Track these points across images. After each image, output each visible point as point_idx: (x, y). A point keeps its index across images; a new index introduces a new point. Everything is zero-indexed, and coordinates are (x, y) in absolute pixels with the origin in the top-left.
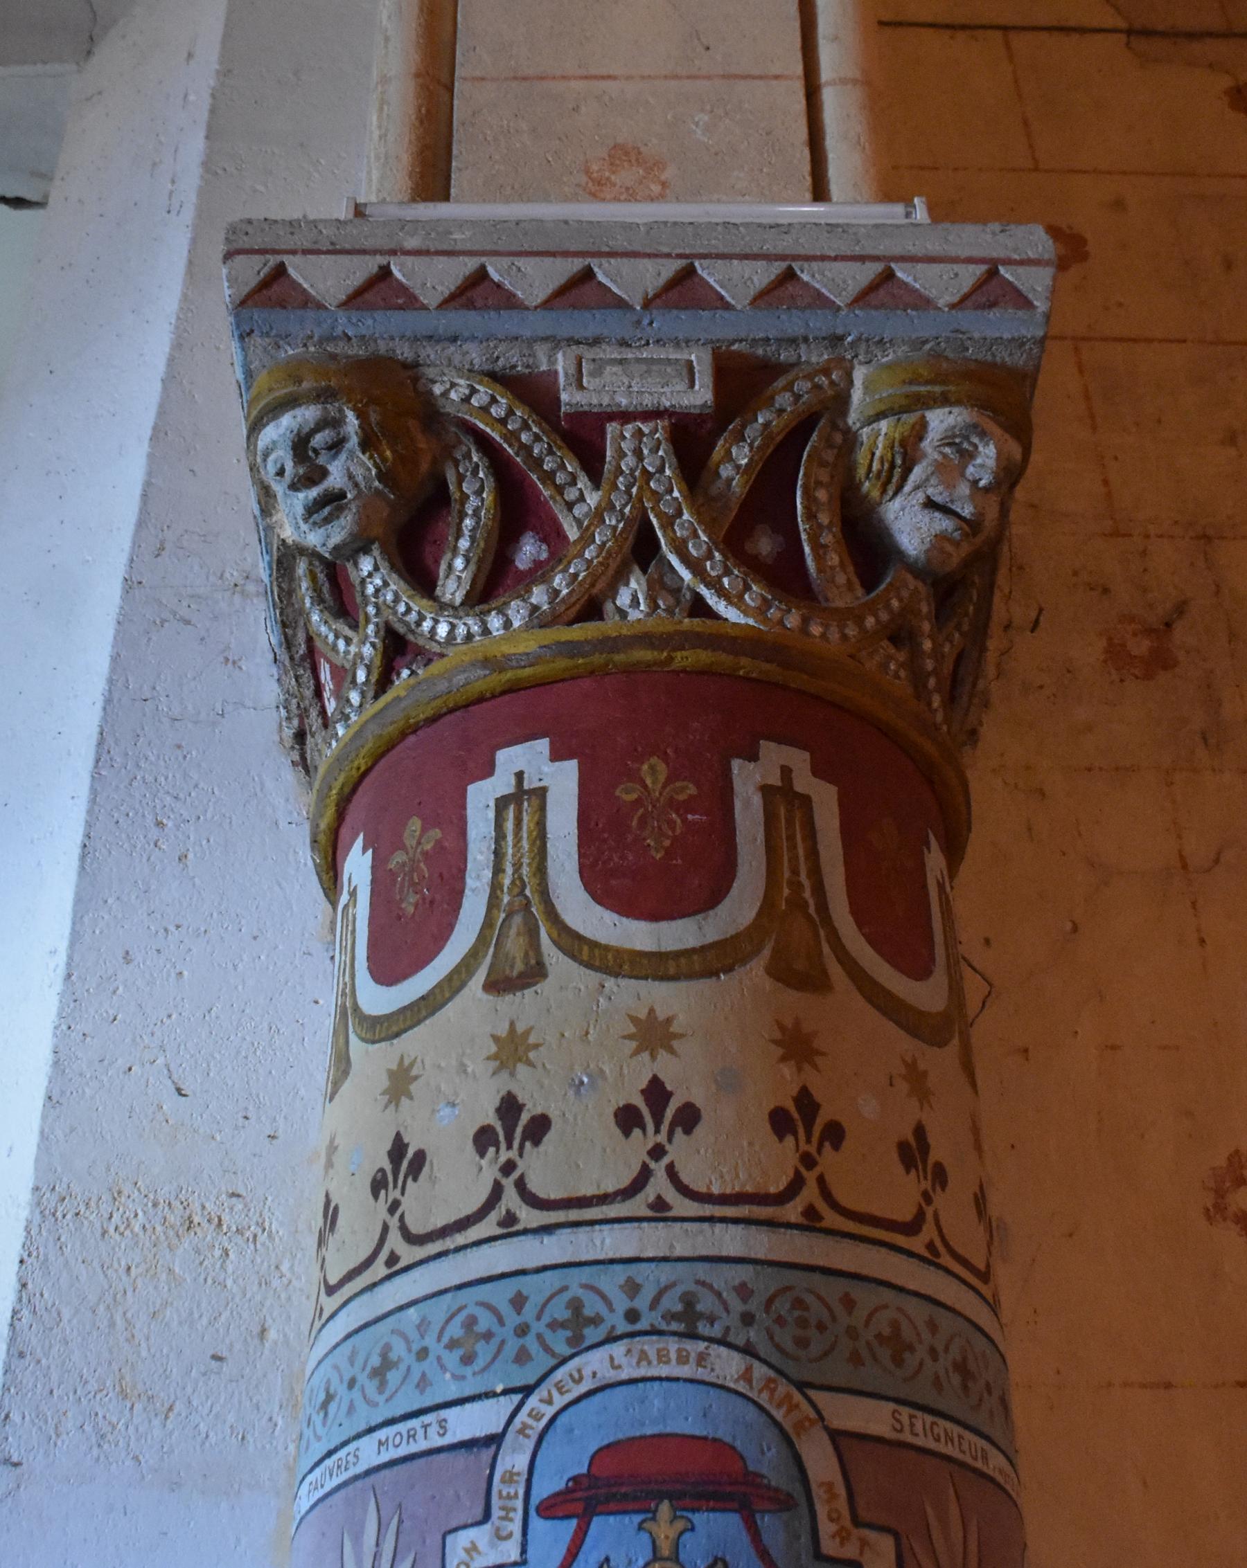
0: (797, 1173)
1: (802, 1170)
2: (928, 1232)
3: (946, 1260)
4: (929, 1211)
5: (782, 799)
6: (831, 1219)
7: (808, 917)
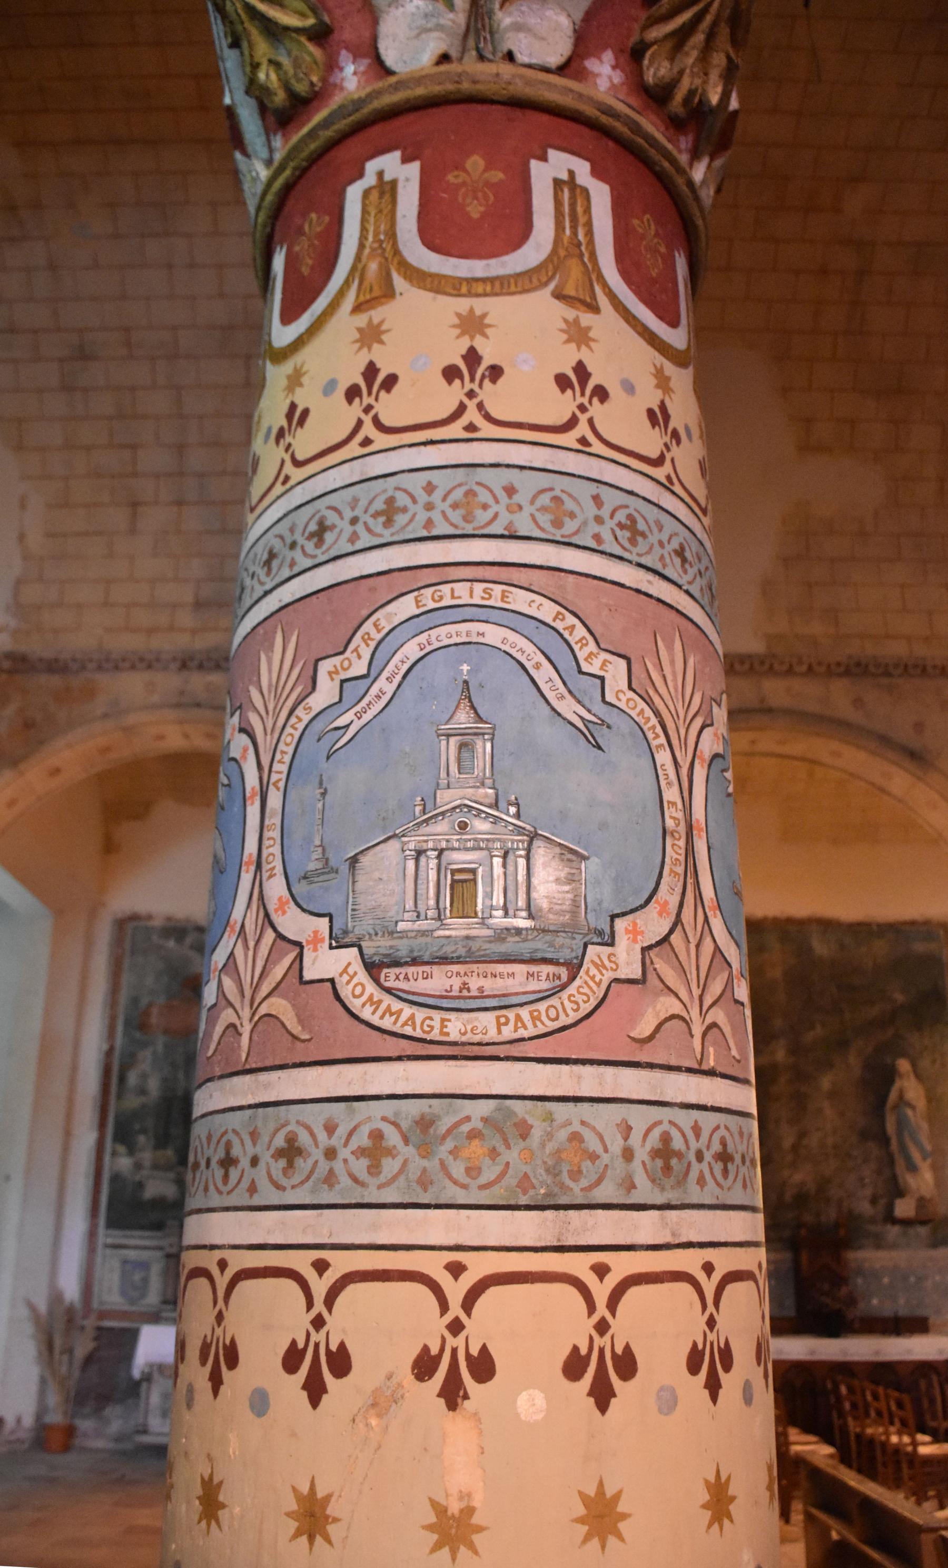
0: (574, 415)
1: (578, 413)
2: (667, 468)
3: (677, 488)
4: (668, 457)
5: (566, 186)
6: (597, 447)
7: (584, 264)
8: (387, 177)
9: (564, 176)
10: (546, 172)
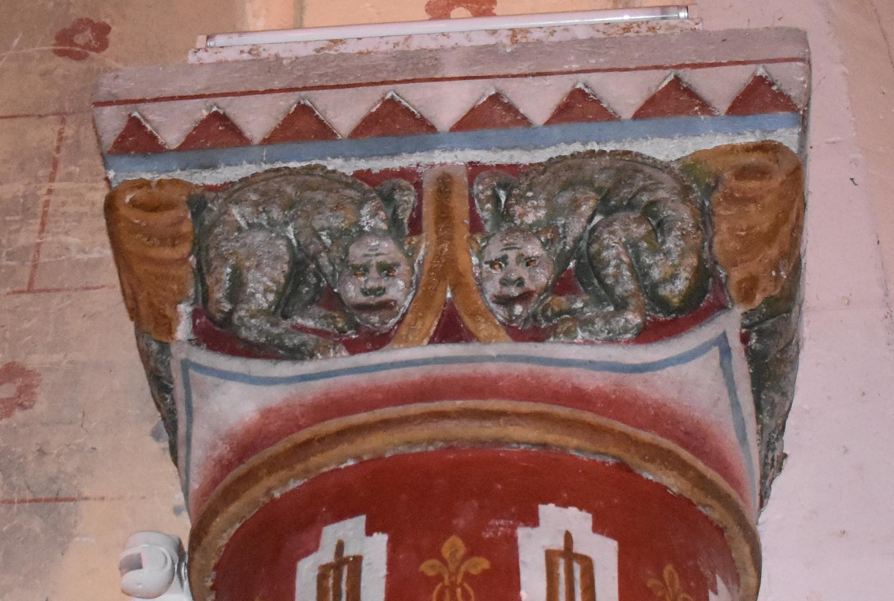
8: (349, 552)
9: (559, 544)
10: (533, 546)
